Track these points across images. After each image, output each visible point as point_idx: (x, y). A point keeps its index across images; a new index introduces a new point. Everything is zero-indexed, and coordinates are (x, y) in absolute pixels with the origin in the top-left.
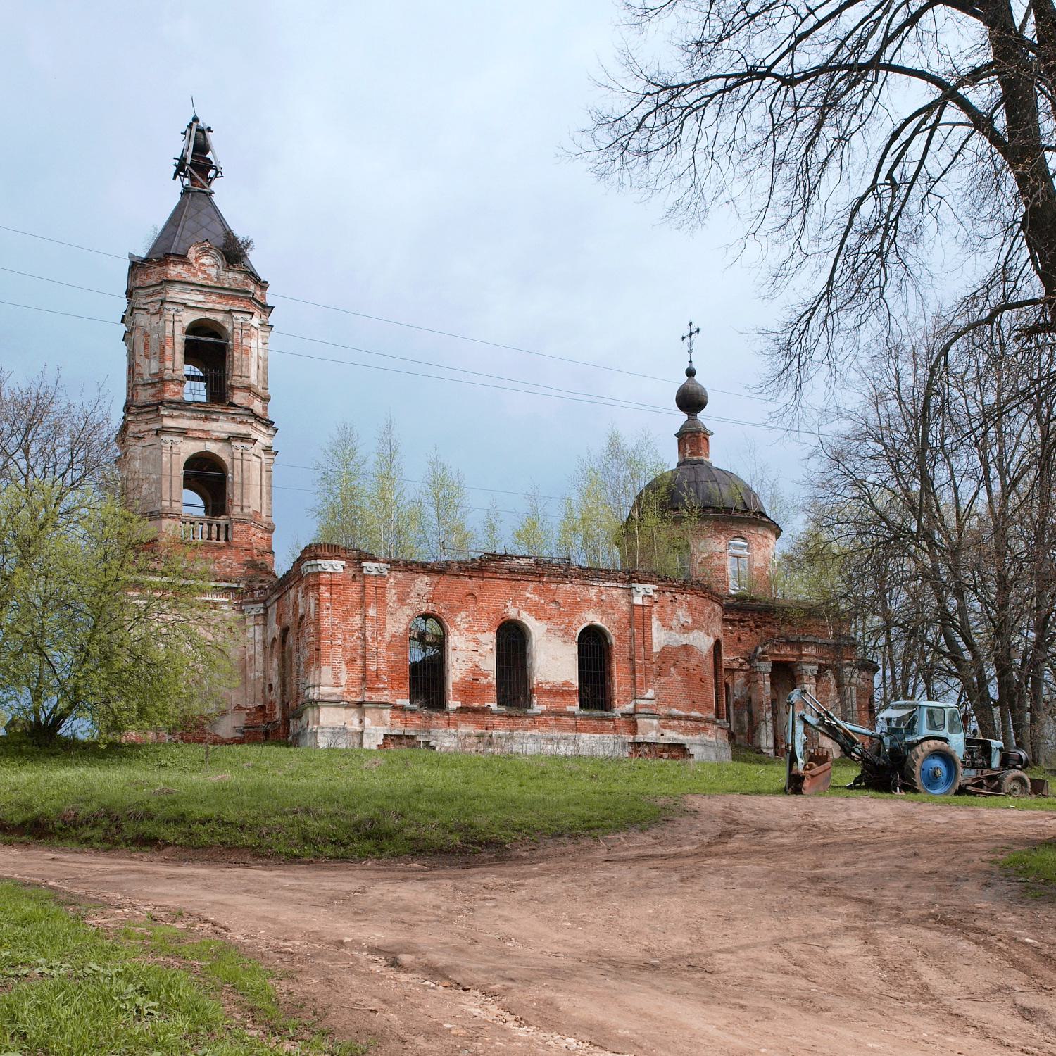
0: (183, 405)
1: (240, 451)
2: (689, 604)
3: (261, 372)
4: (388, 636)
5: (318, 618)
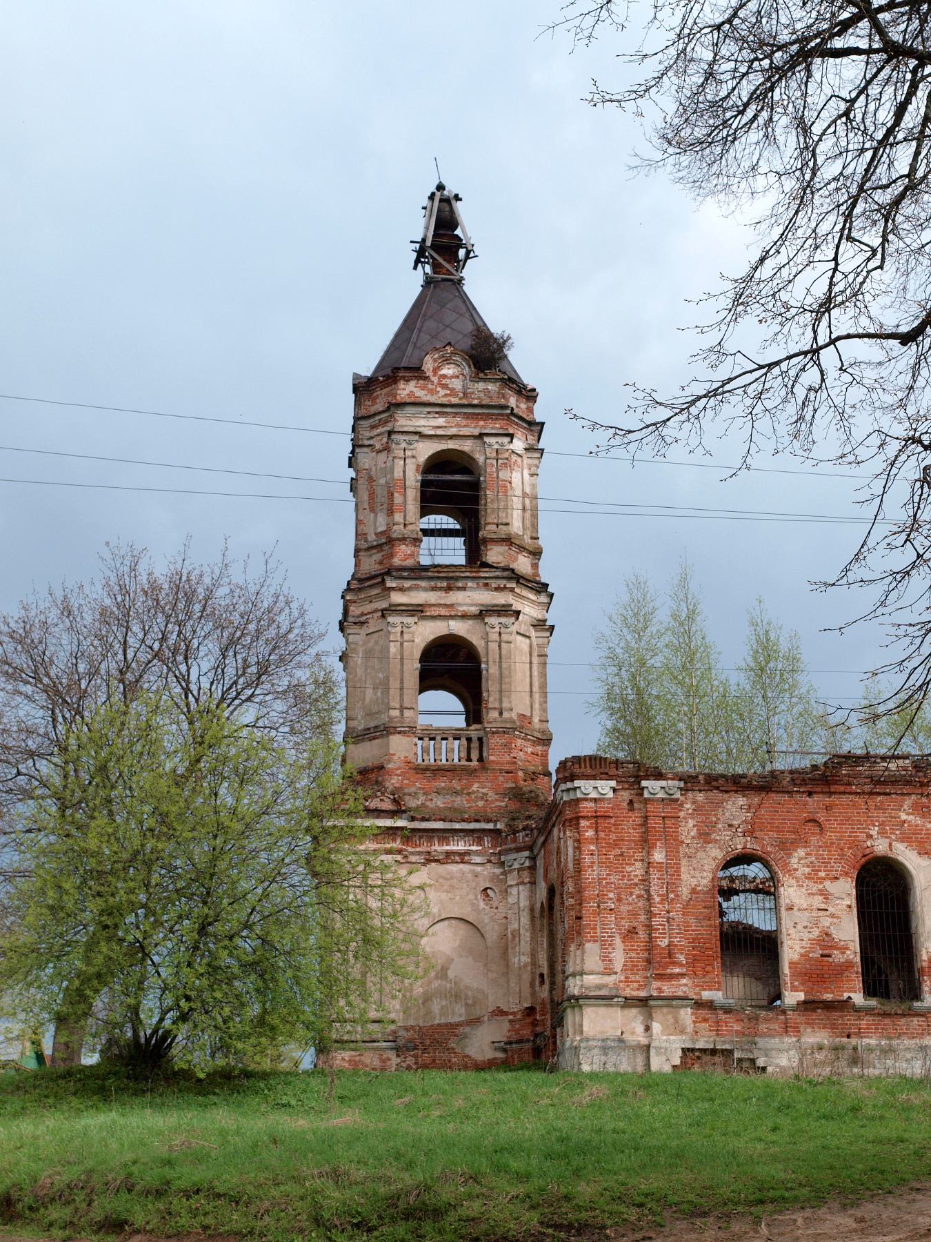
0: (418, 572)
1: (497, 629)
3: (528, 514)
4: (685, 892)
5: (579, 869)
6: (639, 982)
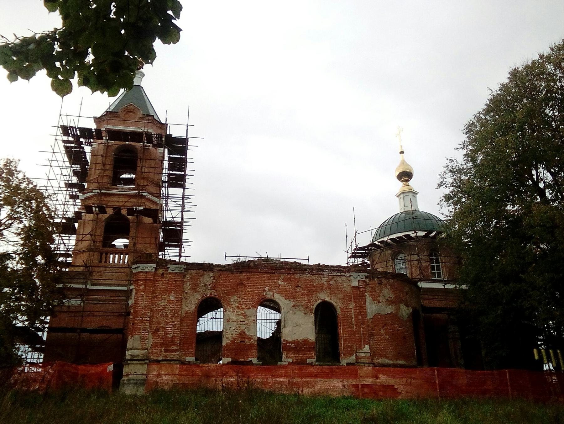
2: (392, 286)
6: (158, 353)
